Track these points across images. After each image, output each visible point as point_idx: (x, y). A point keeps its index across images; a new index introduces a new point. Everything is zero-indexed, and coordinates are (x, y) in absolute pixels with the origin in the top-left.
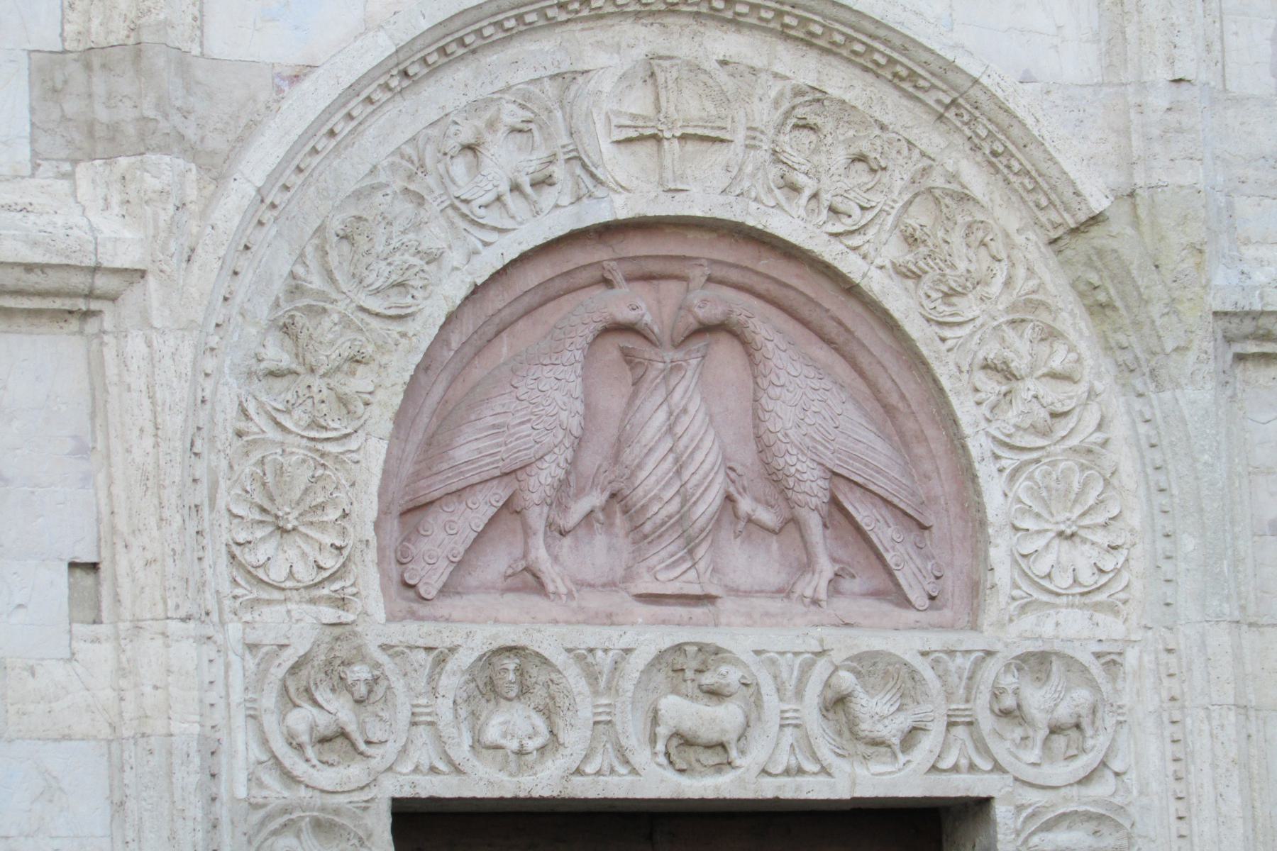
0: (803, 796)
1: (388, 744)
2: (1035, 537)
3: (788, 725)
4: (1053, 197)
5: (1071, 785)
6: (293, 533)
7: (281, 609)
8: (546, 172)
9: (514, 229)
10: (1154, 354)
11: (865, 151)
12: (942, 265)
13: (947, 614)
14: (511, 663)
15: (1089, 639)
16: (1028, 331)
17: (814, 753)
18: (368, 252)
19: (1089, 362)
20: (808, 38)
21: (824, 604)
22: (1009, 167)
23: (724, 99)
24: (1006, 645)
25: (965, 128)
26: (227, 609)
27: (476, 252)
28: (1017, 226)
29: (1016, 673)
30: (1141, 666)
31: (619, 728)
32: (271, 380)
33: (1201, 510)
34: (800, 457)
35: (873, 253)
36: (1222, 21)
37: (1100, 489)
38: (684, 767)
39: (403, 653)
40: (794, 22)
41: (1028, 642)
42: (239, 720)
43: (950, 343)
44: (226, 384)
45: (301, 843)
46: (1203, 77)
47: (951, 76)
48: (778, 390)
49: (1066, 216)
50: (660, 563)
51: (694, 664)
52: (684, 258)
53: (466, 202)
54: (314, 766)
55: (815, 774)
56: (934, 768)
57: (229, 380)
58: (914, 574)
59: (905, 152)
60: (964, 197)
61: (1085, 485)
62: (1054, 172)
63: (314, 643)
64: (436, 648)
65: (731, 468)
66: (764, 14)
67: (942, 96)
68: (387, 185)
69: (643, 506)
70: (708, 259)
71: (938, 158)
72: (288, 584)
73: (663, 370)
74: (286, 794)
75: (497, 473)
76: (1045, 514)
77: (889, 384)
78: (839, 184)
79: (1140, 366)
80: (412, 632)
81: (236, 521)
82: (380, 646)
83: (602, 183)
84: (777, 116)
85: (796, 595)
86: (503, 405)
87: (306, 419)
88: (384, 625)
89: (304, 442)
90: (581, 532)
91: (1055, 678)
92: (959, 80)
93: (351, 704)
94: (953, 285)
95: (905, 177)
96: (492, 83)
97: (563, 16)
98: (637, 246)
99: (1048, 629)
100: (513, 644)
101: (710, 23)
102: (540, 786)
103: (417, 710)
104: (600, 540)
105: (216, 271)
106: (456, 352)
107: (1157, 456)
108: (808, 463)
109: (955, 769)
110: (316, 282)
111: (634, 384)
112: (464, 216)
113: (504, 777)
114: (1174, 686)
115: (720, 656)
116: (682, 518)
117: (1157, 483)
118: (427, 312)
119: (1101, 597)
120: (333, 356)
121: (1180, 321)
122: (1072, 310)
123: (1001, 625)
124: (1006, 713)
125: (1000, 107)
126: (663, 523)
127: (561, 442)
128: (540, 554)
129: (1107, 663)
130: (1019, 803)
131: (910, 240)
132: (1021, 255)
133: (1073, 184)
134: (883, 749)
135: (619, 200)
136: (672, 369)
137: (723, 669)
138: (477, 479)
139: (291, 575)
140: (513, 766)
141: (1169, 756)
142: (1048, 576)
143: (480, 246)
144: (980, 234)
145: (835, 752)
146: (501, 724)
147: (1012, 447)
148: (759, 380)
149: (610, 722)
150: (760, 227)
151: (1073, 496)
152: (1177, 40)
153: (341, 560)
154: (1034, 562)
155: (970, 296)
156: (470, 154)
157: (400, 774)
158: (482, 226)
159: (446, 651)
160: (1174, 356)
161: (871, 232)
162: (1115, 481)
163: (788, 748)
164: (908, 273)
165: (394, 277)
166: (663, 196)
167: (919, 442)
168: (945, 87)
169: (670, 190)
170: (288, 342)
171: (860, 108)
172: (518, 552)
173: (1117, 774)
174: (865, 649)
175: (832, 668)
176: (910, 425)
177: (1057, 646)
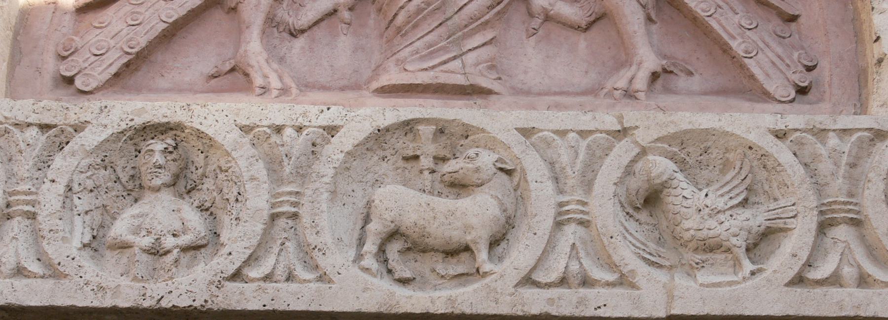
21: (641, 95)
31: (306, 219)
38: (408, 274)
50: (412, 55)
55: (609, 284)
56: (799, 280)
58: (773, 63)
64: (55, 126)
85: (605, 91)
90: (319, 32)
100: (165, 120)
102: (175, 293)
104: (344, 42)
109: (834, 280)
113: (125, 282)
134: (719, 257)
137: (471, 152)
140: (140, 270)
145: (644, 259)
146: (133, 216)
149: (295, 216)
159: (71, 130)
174: (685, 126)
175: (637, 150)
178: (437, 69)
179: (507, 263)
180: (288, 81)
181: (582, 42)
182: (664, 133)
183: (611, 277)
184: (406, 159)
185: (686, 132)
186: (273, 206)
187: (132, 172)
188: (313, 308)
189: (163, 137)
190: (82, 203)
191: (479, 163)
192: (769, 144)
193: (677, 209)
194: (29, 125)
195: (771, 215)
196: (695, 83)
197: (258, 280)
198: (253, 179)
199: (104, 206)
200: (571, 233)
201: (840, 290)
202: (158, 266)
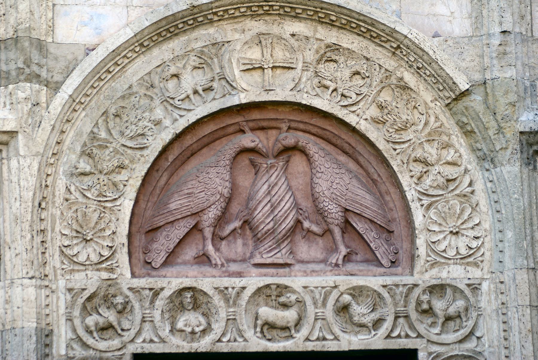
1: (131, 330)
2: (439, 234)
3: (319, 319)
5: (456, 343)
6: (91, 241)
7: (84, 274)
8: (210, 85)
10: (492, 151)
11: (359, 70)
12: (395, 117)
13: (400, 269)
14: (189, 295)
15: (464, 278)
16: (436, 144)
17: (331, 331)
18: (127, 121)
19: (465, 157)
20: (331, 23)
21: (341, 266)
22: (425, 73)
23: (293, 50)
25: (405, 58)
27: (176, 120)
28: (431, 99)
29: (429, 294)
30: (489, 290)
31: (238, 321)
32: (83, 177)
33: (514, 219)
34: (330, 203)
35: (361, 114)
36: (531, 6)
37: (470, 212)
38: (270, 338)
39: (139, 291)
40: (323, 16)
41: (434, 280)
42: (63, 321)
43: (398, 151)
44: (61, 179)
46: (517, 30)
47: (394, 35)
48: (320, 174)
49: (451, 93)
51: (275, 293)
52: (277, 119)
53: (172, 98)
54: (97, 340)
56: (388, 337)
59: (378, 69)
60: (406, 88)
61: (462, 210)
62: (443, 74)
63: (98, 288)
65: (301, 209)
66: (309, 13)
68: (136, 93)
70: (288, 119)
71: (393, 72)
72: (87, 263)
73: (267, 167)
74: (84, 352)
75: (189, 213)
76: (444, 223)
77: (373, 170)
78: (346, 85)
79: (486, 157)
81: (64, 237)
83: (235, 88)
84: (317, 57)
86: (192, 185)
87: (96, 193)
89: (96, 202)
90: (231, 238)
91: (447, 296)
92: (398, 36)
93: (116, 314)
94: (400, 126)
95: (377, 80)
96: (185, 48)
97: (216, 18)
98: (256, 115)
99: (444, 275)
100: (190, 286)
101: (287, 18)
102: (201, 347)
103: (145, 315)
104: (240, 242)
105: (50, 131)
106: (171, 163)
107: (495, 197)
108: (334, 205)
109: (399, 336)
110: (103, 135)
111: (255, 174)
112: (172, 105)
113: (185, 343)
114: (503, 298)
115: (288, 289)
117: (496, 209)
118: (153, 146)
119: (471, 259)
120: (110, 166)
121: (504, 137)
123: (422, 273)
124: (424, 312)
126: (266, 233)
127: (219, 199)
128: (210, 248)
129: (473, 289)
130: (430, 351)
131: (380, 107)
132: (432, 112)
133: (452, 79)
134: (365, 329)
135: (242, 95)
136: (271, 167)
137: (288, 295)
138: (180, 217)
139: (88, 258)
140: (189, 339)
141: (501, 329)
142: (444, 251)
143: (178, 117)
144: (413, 103)
147: (428, 195)
148: (313, 171)
149: (235, 319)
150: (308, 104)
151: (457, 216)
152: (503, 14)
153: (111, 252)
154: (438, 245)
155: (409, 130)
156: (175, 80)
157: (137, 343)
158: (180, 109)
160: (500, 152)
161: (362, 104)
162: (478, 209)
163: (319, 329)
164: (379, 122)
165: (139, 132)
166: (263, 93)
167: (387, 195)
168: (393, 40)
169: (266, 90)
170: (91, 160)
171: (357, 51)
172: (201, 247)
173: (478, 338)
174: (355, 284)
175: (340, 294)
176: (383, 188)
177: (448, 281)
180: (223, 260)
181: (320, 241)
182: (348, 287)
184: (267, 296)
185: (355, 286)
186: (228, 316)
188: (243, 351)
194: (146, 288)
195: (381, 314)
196: (359, 258)
198: (220, 307)
200: (319, 324)
202: (194, 337)
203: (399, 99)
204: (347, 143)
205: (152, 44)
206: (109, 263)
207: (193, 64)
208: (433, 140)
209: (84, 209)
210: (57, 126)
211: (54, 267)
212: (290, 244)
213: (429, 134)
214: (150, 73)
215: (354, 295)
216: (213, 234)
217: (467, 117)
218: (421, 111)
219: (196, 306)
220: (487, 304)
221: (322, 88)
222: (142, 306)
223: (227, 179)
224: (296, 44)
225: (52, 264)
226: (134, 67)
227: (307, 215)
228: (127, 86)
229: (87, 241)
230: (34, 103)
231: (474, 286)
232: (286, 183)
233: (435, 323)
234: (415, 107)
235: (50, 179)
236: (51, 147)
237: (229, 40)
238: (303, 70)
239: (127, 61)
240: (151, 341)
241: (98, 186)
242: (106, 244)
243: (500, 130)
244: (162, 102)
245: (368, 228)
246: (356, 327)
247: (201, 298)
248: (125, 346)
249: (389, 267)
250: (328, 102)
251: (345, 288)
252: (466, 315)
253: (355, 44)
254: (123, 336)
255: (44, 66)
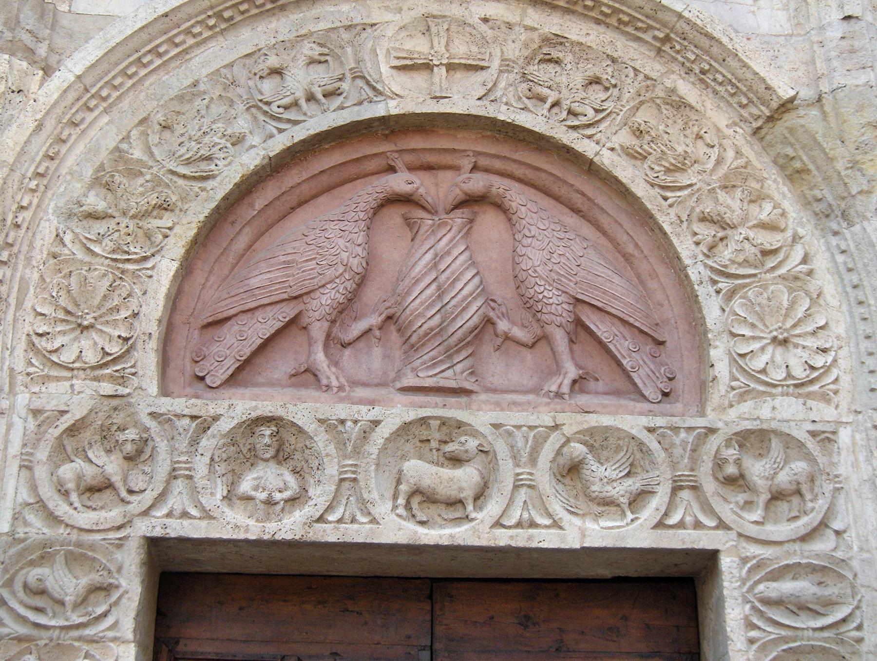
0: (534, 545)
1: (147, 492)
2: (751, 342)
3: (522, 485)
4: (751, 95)
5: (794, 541)
6: (91, 330)
7: (67, 384)
8: (337, 85)
9: (305, 121)
10: (843, 198)
11: (598, 74)
12: (663, 148)
13: (679, 406)
15: (804, 420)
16: (738, 193)
17: (547, 509)
18: (182, 135)
21: (566, 397)
22: (715, 80)
24: (727, 424)
26: (19, 383)
27: (271, 136)
29: (737, 447)
30: (854, 443)
31: (362, 483)
32: (91, 222)
34: (547, 287)
35: (604, 140)
37: (807, 306)
39: (170, 420)
41: (746, 422)
42: (13, 467)
43: (670, 201)
44: (49, 220)
45: (53, 572)
47: (660, 15)
48: (529, 240)
49: (763, 108)
51: (437, 436)
53: (268, 103)
54: (76, 509)
55: (547, 527)
56: (660, 525)
57: (52, 218)
59: (632, 74)
60: (681, 105)
61: (793, 304)
62: (749, 75)
63: (91, 411)
64: (201, 417)
65: (493, 300)
67: (657, 33)
68: (205, 93)
69: (410, 322)
71: (659, 79)
72: (76, 365)
73: (433, 225)
74: (45, 530)
75: (285, 296)
76: (760, 326)
77: (625, 237)
79: (833, 211)
80: (178, 404)
81: (40, 317)
82: (150, 414)
84: (526, 53)
85: (544, 392)
86: (294, 248)
88: (156, 397)
89: (107, 262)
90: (361, 345)
91: (774, 453)
94: (673, 162)
95: (631, 90)
96: (297, 30)
98: (416, 142)
99: (765, 412)
100: (270, 414)
102: (284, 530)
103: (177, 466)
104: (377, 352)
105: (31, 129)
109: (681, 525)
110: (137, 153)
111: (412, 240)
112: (265, 113)
113: (251, 522)
115: (462, 429)
116: (440, 329)
117: (856, 298)
118: (224, 174)
119: (815, 388)
120: (143, 203)
121: (864, 175)
122: (775, 179)
123: (722, 409)
125: (701, 33)
126: (427, 334)
127: (341, 274)
129: (823, 440)
130: (743, 555)
131: (637, 133)
133: (763, 80)
134: (613, 509)
135: (392, 104)
136: (439, 225)
137: (463, 439)
139: (79, 358)
140: (260, 514)
142: (764, 371)
143: (275, 131)
144: (696, 129)
146: (254, 479)
147: (728, 276)
148: (516, 237)
149: (355, 480)
150: (510, 121)
151: (784, 312)
154: (750, 360)
156: (277, 79)
157: (154, 517)
159: (210, 419)
160: (859, 197)
161: (603, 126)
162: (822, 302)
165: (202, 152)
166: (429, 101)
167: (652, 279)
168: (658, 26)
169: (436, 98)
170: (110, 196)
171: (595, 47)
173: (838, 533)
174: (594, 424)
175: (564, 440)
176: (644, 267)
177: (774, 425)
178: (438, 376)
179: (485, 512)
180: (343, 381)
181: (528, 355)
183: (547, 522)
184: (422, 441)
185: (594, 427)
186: (341, 473)
187: (249, 447)
188: (368, 541)
189: (268, 424)
190: (221, 469)
191: (467, 447)
192: (644, 436)
193: (588, 478)
194: (184, 416)
196: (600, 386)
197: (334, 522)
198: (327, 455)
199: (233, 470)
200: (523, 494)
201: (684, 531)
202: (271, 512)
203: (670, 122)
204: (578, 191)
205: (239, 18)
206: (118, 368)
207: (309, 53)
208: (734, 186)
209: (85, 273)
210: (50, 125)
211: (12, 370)
212: (470, 359)
213: (726, 177)
214: (231, 65)
215: (592, 446)
216: (328, 336)
217: (791, 145)
218: (709, 141)
219: (281, 456)
220: (850, 468)
221: (534, 101)
222: (173, 450)
223: (359, 242)
224: (489, 33)
225: (7, 363)
226: (205, 54)
227: (505, 311)
228: (189, 82)
229: (84, 329)
230: (14, 88)
231: (823, 436)
232: (467, 254)
233: (751, 502)
234: (699, 137)
235: (27, 215)
236: (33, 160)
237: (374, 22)
238: (501, 71)
239: (191, 41)
240: (185, 515)
241: (116, 235)
242: (117, 333)
243: (854, 165)
244: (248, 109)
245: (617, 333)
246: (595, 506)
247: (292, 440)
248: (130, 522)
249: (659, 402)
250: (545, 120)
251: (575, 429)
252: (812, 490)
253: (591, 37)
254: (128, 503)
255: (44, 39)
